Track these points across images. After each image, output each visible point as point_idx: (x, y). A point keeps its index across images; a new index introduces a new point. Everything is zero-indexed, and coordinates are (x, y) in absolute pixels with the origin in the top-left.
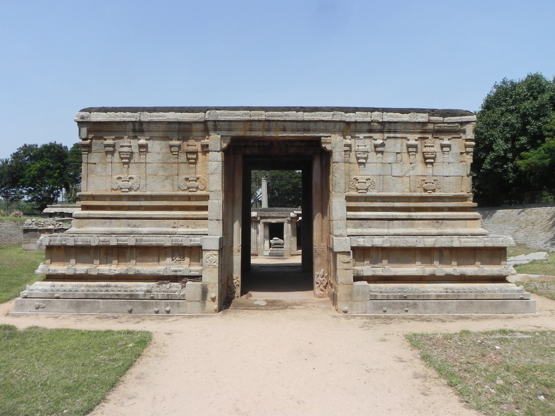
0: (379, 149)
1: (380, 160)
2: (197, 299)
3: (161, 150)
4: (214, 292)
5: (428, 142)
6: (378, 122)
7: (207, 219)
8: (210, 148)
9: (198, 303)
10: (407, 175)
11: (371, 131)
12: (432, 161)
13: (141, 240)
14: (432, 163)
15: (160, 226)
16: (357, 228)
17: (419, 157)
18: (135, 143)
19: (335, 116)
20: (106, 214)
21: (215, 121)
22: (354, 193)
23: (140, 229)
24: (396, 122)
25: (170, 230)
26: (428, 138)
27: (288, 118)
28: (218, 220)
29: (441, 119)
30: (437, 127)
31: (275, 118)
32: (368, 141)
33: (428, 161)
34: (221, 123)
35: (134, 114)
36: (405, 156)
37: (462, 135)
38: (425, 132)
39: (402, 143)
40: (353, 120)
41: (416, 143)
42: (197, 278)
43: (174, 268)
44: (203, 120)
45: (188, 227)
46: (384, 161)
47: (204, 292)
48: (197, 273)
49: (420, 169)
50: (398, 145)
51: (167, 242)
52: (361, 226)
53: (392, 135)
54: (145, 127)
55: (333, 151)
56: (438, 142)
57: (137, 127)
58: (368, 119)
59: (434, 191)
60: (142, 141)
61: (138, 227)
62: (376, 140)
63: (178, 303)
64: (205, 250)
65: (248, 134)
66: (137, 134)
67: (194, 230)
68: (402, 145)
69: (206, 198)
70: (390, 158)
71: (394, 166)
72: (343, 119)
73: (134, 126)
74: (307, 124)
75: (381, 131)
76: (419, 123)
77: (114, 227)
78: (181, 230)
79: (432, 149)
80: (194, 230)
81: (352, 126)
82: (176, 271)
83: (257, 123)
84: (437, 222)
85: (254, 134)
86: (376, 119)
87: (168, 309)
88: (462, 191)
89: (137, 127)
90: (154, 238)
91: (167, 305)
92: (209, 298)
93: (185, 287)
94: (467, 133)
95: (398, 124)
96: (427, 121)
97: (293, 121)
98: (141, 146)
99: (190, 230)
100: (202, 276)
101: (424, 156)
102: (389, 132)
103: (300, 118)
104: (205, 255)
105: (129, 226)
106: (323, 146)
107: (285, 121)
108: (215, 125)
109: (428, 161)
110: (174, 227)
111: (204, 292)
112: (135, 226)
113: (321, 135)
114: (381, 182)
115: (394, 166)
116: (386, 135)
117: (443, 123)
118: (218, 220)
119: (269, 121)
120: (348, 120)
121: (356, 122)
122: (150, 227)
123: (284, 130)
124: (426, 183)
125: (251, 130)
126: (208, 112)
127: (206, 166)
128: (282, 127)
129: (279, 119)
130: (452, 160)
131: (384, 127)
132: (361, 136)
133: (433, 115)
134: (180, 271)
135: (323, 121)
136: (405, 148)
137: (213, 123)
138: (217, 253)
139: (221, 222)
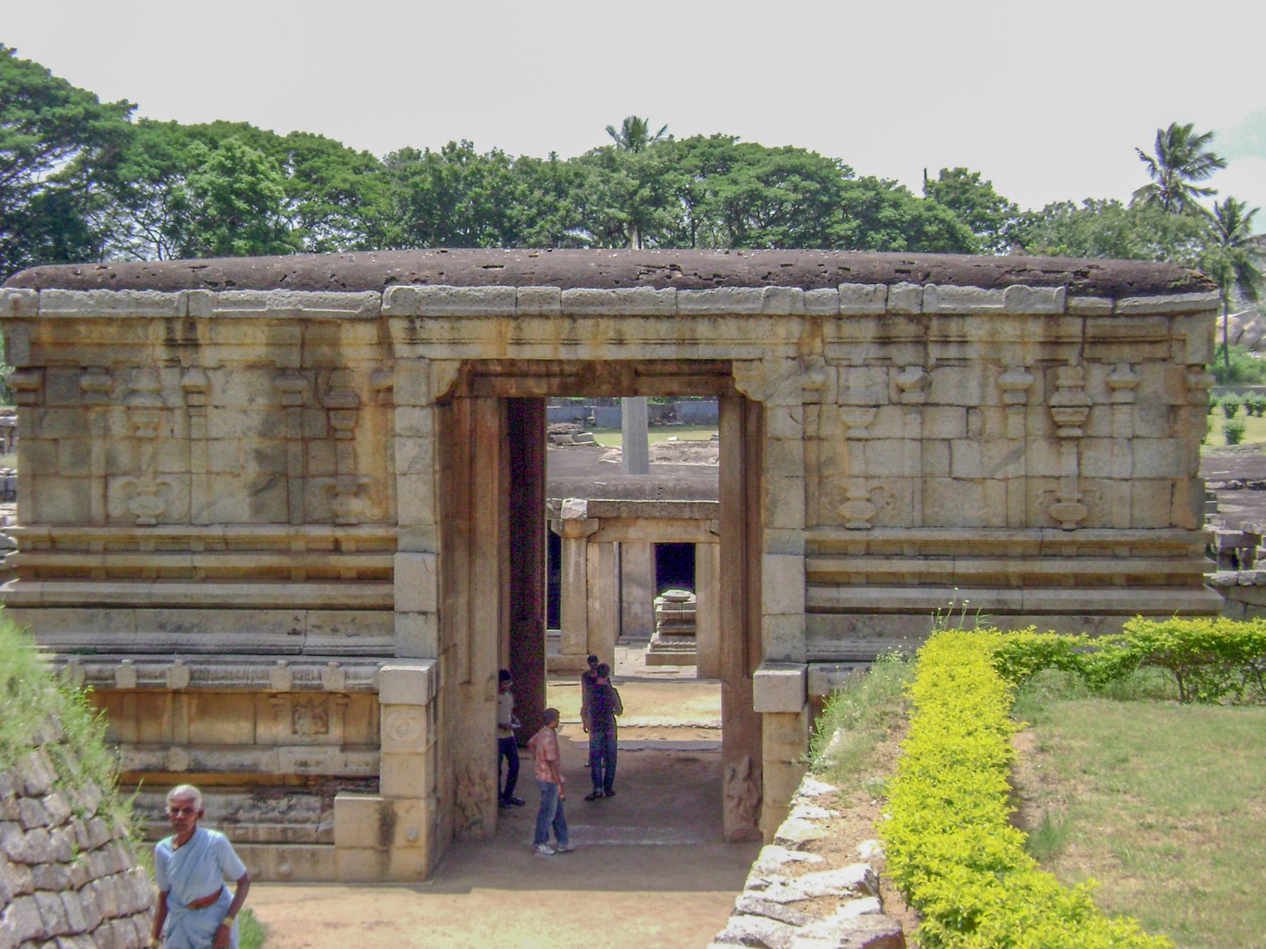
0: (914, 397)
1: (914, 430)
2: (366, 843)
3: (251, 400)
4: (415, 820)
5: (1066, 376)
6: (911, 318)
7: (390, 608)
8: (397, 398)
9: (371, 852)
10: (999, 475)
11: (884, 341)
12: (1077, 432)
13: (205, 675)
14: (1076, 439)
15: (251, 629)
16: (838, 637)
17: (1038, 423)
18: (170, 378)
19: (773, 303)
20: (95, 595)
21: (411, 319)
22: (831, 535)
23: (196, 638)
24: (962, 316)
25: (284, 640)
26: (1065, 363)
27: (628, 309)
28: (424, 613)
29: (1106, 303)
30: (1093, 328)
31: (590, 310)
32: (878, 374)
33: (1063, 433)
34: (430, 324)
35: (168, 295)
36: (993, 421)
37: (1176, 347)
38: (1056, 342)
39: (985, 378)
40: (829, 310)
41: (1028, 379)
42: (368, 783)
43: (301, 754)
44: (373, 315)
45: (335, 631)
46: (927, 433)
47: (387, 824)
48: (364, 770)
49: (1042, 459)
50: (973, 385)
51: (279, 677)
52: (853, 629)
53: (953, 352)
54: (202, 332)
55: (769, 404)
56: (1098, 375)
57: (179, 335)
58: (877, 307)
59: (1082, 525)
60: (194, 379)
61: (189, 630)
62: (902, 369)
63: (313, 854)
64: (387, 706)
65: (511, 353)
66: (181, 353)
67: (352, 641)
68: (983, 385)
69: (389, 546)
70: (947, 424)
71: (960, 447)
72: (800, 308)
73: (170, 330)
74: (688, 324)
75: (921, 342)
76: (1036, 316)
77: (118, 629)
78: (314, 640)
79: (1080, 398)
80: (352, 641)
81: (829, 329)
82: (304, 764)
83: (536, 323)
84: (1087, 621)
85: (528, 353)
86: (902, 305)
87: (285, 868)
88: (1172, 526)
89: (179, 335)
90: (242, 668)
91: (282, 858)
92: (400, 838)
93: (331, 806)
94: (1189, 349)
95: (969, 320)
96: (1061, 311)
97: (646, 317)
98: (187, 392)
99: (341, 641)
100: (378, 777)
101: (1050, 417)
102: (945, 342)
103: (665, 309)
104: (389, 722)
105: (162, 627)
106: (739, 387)
107: (622, 317)
108: (412, 330)
109: (1063, 433)
110: (295, 632)
111: (387, 824)
112: (179, 629)
113: (733, 355)
114: (918, 496)
115: (960, 447)
116: (935, 352)
117: (1113, 315)
118: (424, 613)
119: (573, 317)
120: (815, 310)
121: (839, 317)
122: (224, 630)
123: (620, 342)
124: (1059, 501)
125: (518, 342)
126: (391, 289)
127: (386, 450)
128: (611, 334)
129: (603, 310)
130: (1142, 429)
131: (927, 328)
132: (857, 355)
133: (1082, 292)
134: (318, 763)
135: (738, 316)
136: (992, 397)
137: (405, 324)
138: (421, 715)
139: (433, 619)
